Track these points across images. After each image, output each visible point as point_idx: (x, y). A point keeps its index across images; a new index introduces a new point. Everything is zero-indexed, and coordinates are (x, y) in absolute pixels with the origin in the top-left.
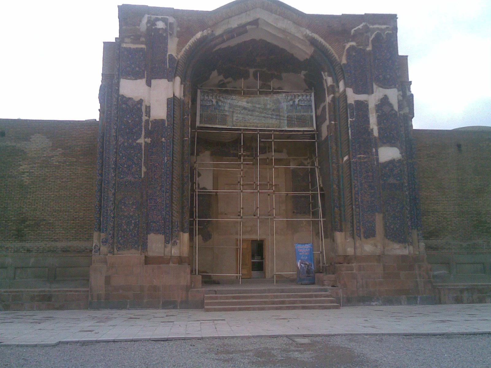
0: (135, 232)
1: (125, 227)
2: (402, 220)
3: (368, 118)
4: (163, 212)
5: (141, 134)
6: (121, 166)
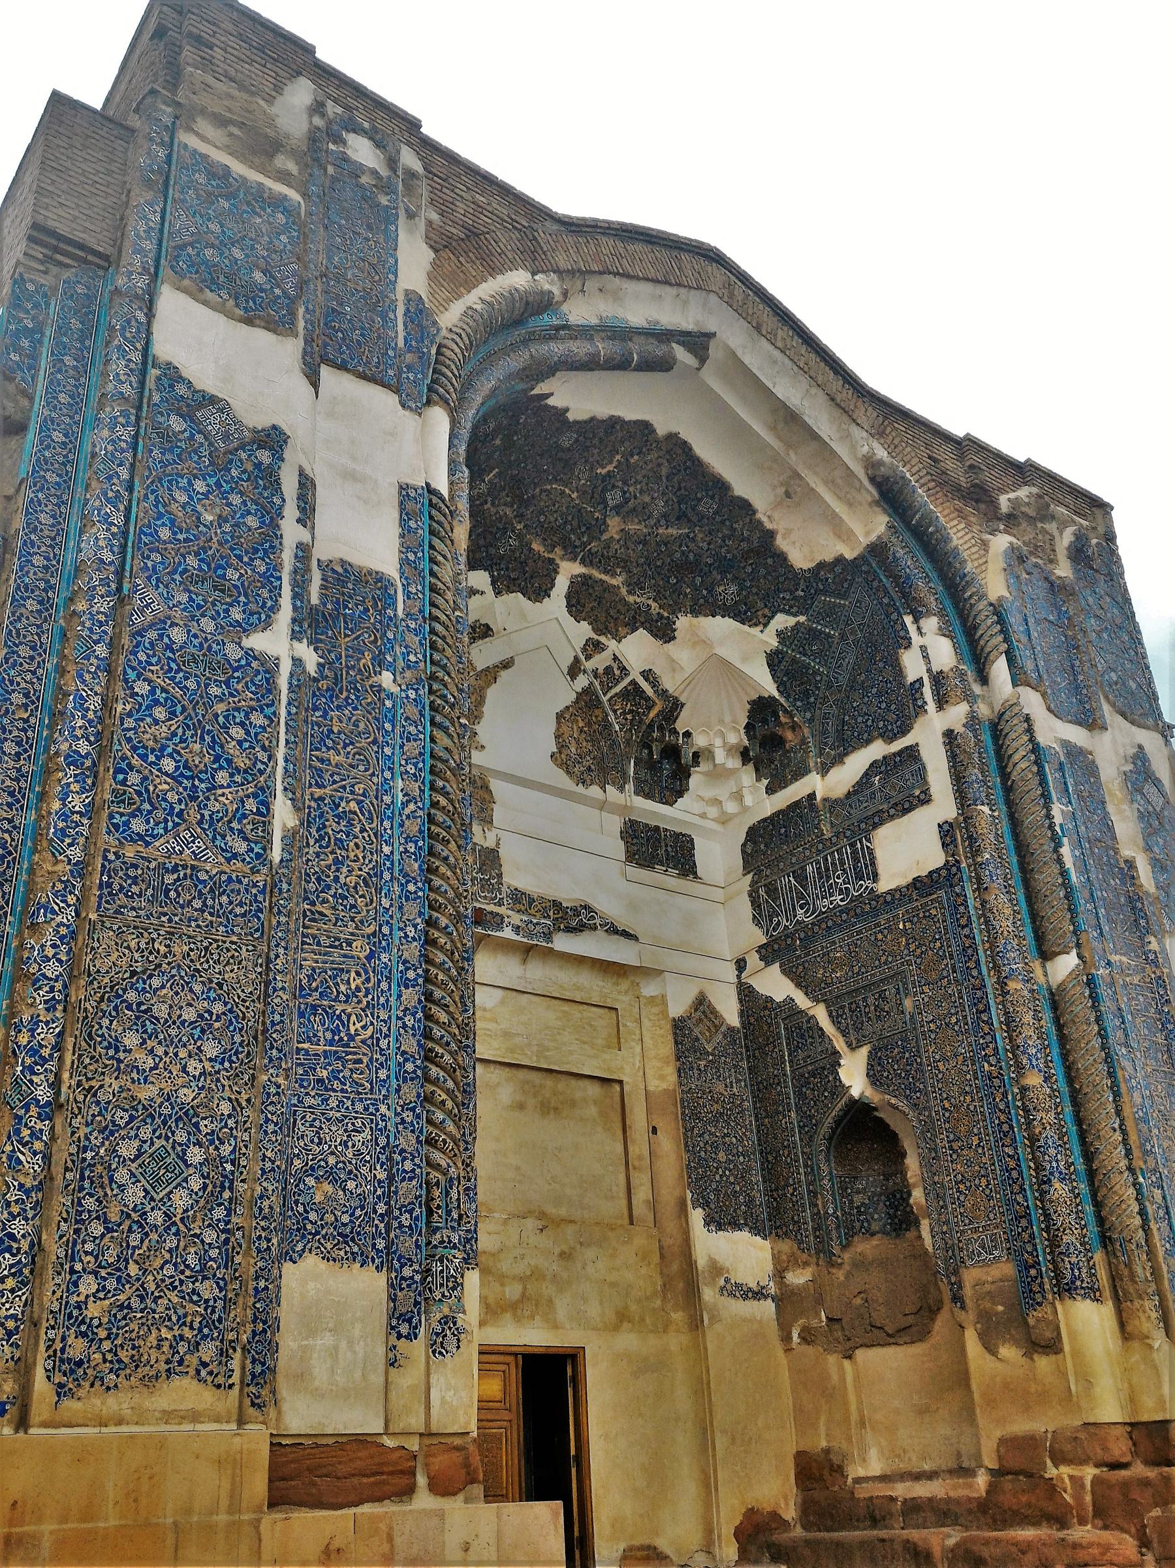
0: (210, 1236)
1: (135, 1195)
3: (1106, 814)
4: (383, 1109)
5: (275, 608)
6: (136, 761)
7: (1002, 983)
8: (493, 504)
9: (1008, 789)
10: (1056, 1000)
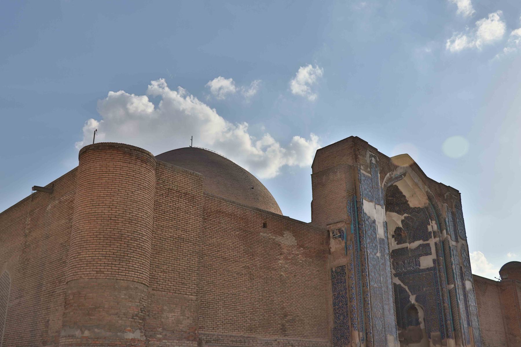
7: (442, 289)
9: (445, 255)
10: (450, 292)
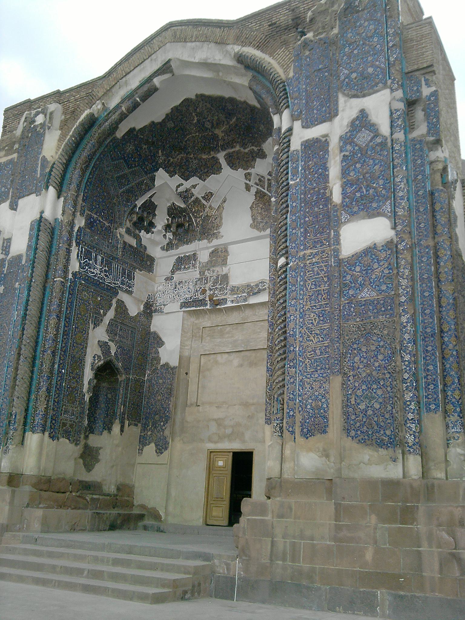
2: (389, 389)
3: (326, 169)
8: (173, 158)
